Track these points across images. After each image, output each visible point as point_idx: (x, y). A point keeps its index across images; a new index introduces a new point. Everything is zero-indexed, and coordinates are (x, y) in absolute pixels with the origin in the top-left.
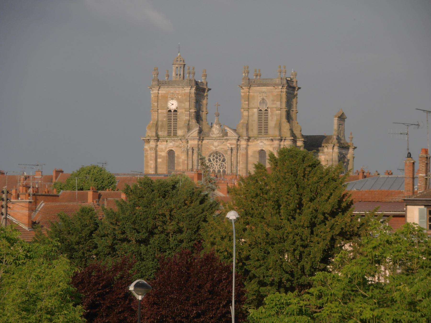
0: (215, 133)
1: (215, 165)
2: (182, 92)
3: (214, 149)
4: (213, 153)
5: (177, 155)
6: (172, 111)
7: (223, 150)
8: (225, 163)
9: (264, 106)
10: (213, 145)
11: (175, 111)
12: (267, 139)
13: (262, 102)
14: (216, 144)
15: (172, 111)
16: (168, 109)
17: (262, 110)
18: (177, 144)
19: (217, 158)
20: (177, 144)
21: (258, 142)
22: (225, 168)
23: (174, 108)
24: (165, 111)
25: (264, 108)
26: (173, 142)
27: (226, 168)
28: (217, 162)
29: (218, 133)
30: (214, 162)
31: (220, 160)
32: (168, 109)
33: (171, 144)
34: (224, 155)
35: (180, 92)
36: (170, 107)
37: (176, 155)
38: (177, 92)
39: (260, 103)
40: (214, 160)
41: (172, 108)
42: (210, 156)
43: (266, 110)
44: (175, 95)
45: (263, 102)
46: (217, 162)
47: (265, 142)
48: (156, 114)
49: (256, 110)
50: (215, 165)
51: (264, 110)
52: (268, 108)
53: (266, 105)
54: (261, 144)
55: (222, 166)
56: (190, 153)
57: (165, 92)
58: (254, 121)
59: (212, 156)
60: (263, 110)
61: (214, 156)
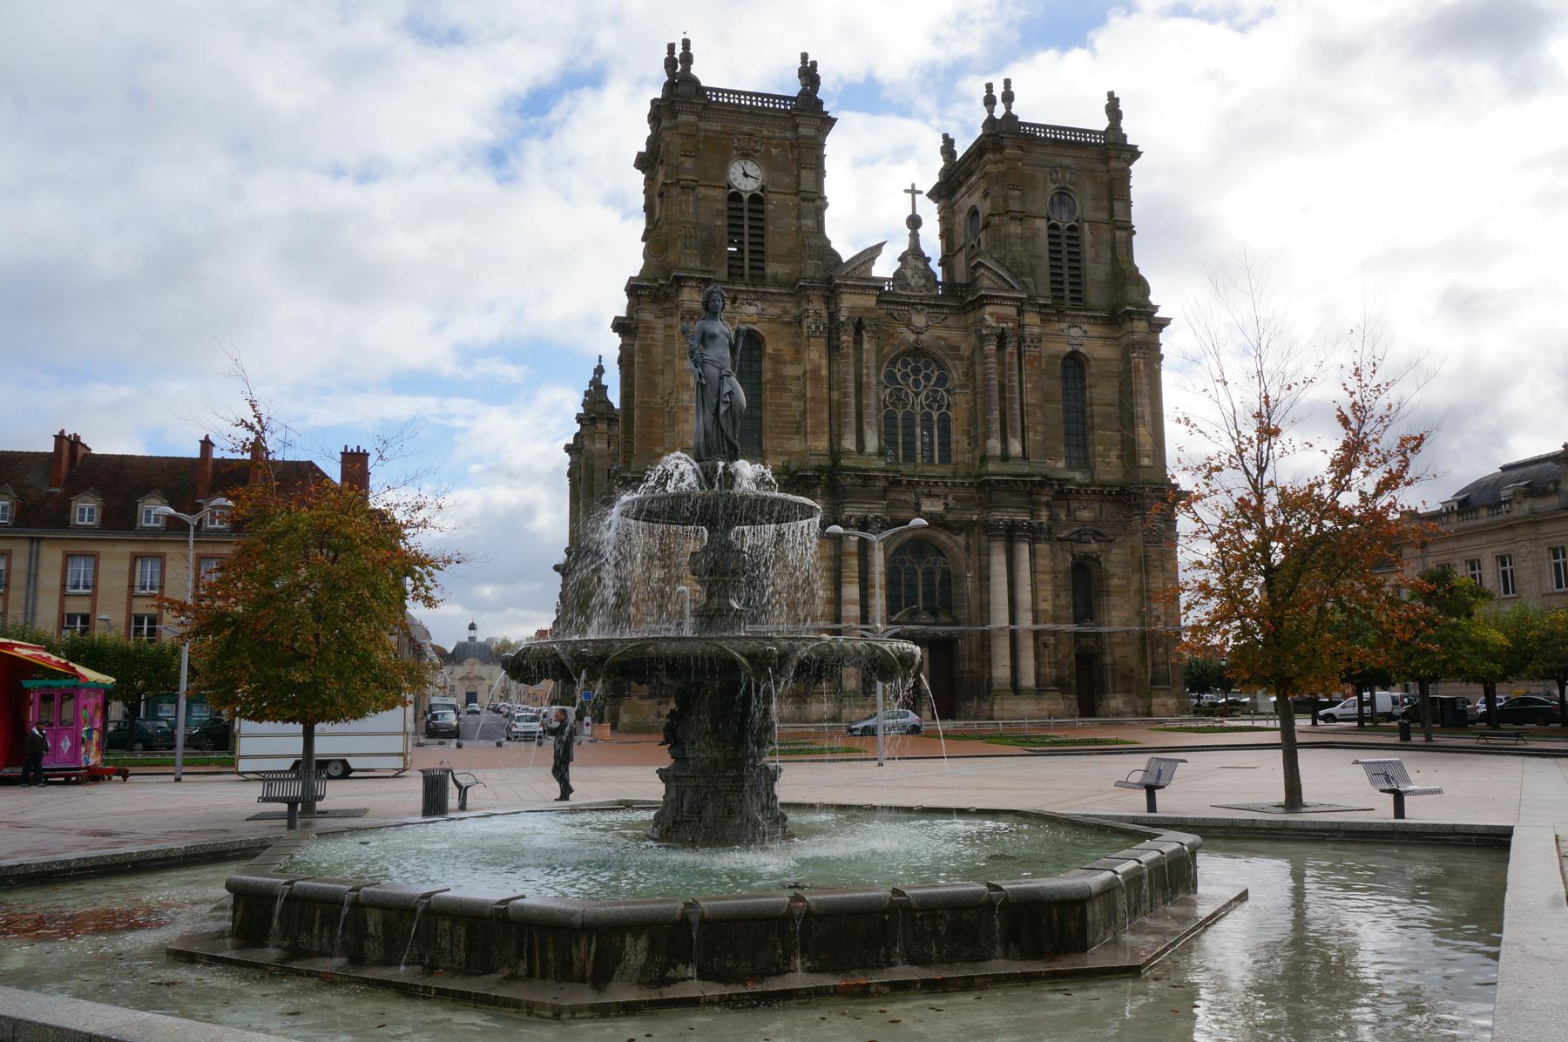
0: (913, 284)
1: (911, 395)
2: (783, 135)
3: (912, 337)
4: (904, 353)
5: (774, 350)
6: (746, 197)
7: (942, 343)
8: (947, 391)
9: (1065, 216)
10: (909, 324)
11: (755, 198)
12: (1094, 317)
13: (1055, 199)
14: (919, 320)
15: (746, 197)
16: (729, 187)
17: (1061, 225)
18: (773, 311)
19: (916, 371)
20: (773, 311)
21: (1064, 325)
22: (948, 408)
23: (749, 188)
24: (719, 194)
25: (1064, 220)
26: (758, 303)
27: (953, 408)
28: (917, 383)
29: (924, 286)
30: (908, 385)
31: (927, 378)
32: (729, 187)
33: (752, 310)
34: (949, 363)
35: (777, 135)
36: (736, 184)
37: (769, 349)
38: (765, 133)
39: (1052, 202)
40: (905, 376)
41: (742, 188)
42: (893, 362)
43: (1071, 228)
44: (756, 142)
45: (1062, 203)
46: (917, 383)
47: (1085, 327)
48: (691, 199)
49: (1042, 224)
50: (911, 395)
51: (1067, 225)
52: (1077, 221)
53: (1072, 211)
54: (1074, 332)
55: (935, 400)
56: (846, 338)
57: (719, 128)
58: (1039, 257)
59: (899, 365)
60: (1064, 226)
61: (905, 365)
